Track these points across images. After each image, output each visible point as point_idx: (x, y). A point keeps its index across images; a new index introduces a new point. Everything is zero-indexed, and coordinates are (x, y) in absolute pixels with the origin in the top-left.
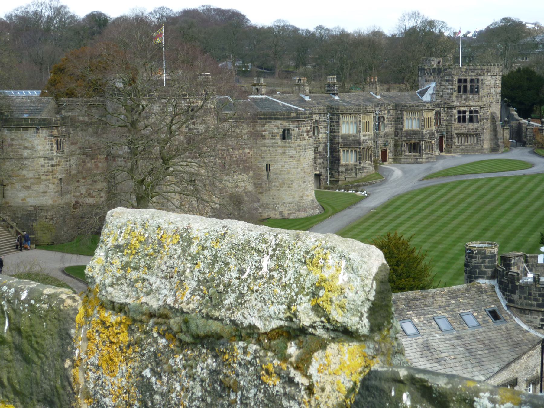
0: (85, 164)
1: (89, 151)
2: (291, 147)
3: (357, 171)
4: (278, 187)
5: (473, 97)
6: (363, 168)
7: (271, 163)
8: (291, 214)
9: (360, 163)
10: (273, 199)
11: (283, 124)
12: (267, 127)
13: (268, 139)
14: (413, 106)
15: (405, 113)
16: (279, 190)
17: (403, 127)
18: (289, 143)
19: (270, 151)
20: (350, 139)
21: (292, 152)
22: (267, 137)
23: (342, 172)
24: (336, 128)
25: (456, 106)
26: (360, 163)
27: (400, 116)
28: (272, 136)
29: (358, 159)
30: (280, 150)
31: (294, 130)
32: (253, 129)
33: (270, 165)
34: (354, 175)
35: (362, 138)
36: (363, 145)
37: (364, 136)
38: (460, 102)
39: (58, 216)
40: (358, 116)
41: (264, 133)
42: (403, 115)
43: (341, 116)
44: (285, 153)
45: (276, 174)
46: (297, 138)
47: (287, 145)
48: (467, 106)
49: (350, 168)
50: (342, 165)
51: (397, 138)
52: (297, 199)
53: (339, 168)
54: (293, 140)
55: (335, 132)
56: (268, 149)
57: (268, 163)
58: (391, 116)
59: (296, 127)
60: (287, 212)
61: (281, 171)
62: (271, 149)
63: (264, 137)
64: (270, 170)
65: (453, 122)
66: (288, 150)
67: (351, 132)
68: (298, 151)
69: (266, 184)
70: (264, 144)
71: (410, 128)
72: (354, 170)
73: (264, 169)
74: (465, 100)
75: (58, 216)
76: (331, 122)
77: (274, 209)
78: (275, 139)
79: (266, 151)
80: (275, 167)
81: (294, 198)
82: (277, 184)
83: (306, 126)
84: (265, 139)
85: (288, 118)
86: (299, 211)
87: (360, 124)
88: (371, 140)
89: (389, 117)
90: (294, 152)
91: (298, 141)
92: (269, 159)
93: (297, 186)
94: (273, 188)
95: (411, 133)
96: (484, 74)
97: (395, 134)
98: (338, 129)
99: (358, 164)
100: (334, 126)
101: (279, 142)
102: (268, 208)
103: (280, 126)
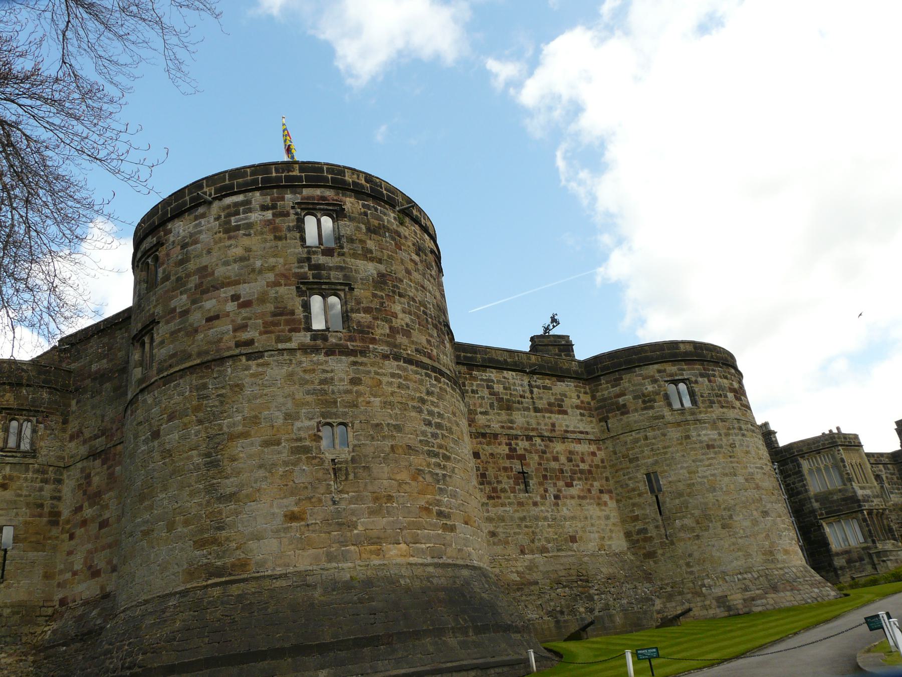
0: (89, 484)
1: (100, 443)
3: (875, 559)
4: (693, 530)
6: (885, 552)
7: (657, 469)
9: (874, 542)
11: (665, 371)
12: (625, 384)
13: (636, 410)
18: (693, 414)
19: (646, 438)
20: (835, 497)
21: (708, 434)
22: (631, 407)
23: (842, 568)
24: (799, 485)
26: (874, 542)
28: (644, 402)
29: (867, 534)
30: (674, 434)
31: (696, 382)
32: (593, 397)
34: (869, 568)
35: (860, 493)
36: (867, 506)
37: (862, 488)
40: (835, 450)
41: (621, 400)
43: (801, 461)
44: (688, 437)
45: (680, 495)
46: (712, 402)
47: (689, 418)
49: (855, 556)
50: (837, 554)
52: (757, 560)
53: (831, 561)
54: (701, 405)
55: (799, 493)
57: (651, 470)
58: (891, 474)
59: (702, 375)
60: (739, 596)
62: (650, 434)
63: (623, 410)
64: (660, 490)
68: (723, 431)
69: (657, 527)
72: (867, 560)
73: (643, 487)
76: (785, 478)
77: (700, 594)
78: (652, 408)
79: (637, 441)
81: (748, 555)
82: (688, 522)
83: (726, 378)
84: (627, 412)
85: (675, 355)
86: (775, 589)
87: (845, 466)
88: (877, 496)
89: (889, 476)
90: (713, 434)
91: (717, 411)
92: (650, 461)
93: (747, 523)
94: (682, 535)
98: (804, 485)
99: (870, 544)
100: (794, 483)
101: (666, 412)
102: (681, 593)
103: (657, 376)
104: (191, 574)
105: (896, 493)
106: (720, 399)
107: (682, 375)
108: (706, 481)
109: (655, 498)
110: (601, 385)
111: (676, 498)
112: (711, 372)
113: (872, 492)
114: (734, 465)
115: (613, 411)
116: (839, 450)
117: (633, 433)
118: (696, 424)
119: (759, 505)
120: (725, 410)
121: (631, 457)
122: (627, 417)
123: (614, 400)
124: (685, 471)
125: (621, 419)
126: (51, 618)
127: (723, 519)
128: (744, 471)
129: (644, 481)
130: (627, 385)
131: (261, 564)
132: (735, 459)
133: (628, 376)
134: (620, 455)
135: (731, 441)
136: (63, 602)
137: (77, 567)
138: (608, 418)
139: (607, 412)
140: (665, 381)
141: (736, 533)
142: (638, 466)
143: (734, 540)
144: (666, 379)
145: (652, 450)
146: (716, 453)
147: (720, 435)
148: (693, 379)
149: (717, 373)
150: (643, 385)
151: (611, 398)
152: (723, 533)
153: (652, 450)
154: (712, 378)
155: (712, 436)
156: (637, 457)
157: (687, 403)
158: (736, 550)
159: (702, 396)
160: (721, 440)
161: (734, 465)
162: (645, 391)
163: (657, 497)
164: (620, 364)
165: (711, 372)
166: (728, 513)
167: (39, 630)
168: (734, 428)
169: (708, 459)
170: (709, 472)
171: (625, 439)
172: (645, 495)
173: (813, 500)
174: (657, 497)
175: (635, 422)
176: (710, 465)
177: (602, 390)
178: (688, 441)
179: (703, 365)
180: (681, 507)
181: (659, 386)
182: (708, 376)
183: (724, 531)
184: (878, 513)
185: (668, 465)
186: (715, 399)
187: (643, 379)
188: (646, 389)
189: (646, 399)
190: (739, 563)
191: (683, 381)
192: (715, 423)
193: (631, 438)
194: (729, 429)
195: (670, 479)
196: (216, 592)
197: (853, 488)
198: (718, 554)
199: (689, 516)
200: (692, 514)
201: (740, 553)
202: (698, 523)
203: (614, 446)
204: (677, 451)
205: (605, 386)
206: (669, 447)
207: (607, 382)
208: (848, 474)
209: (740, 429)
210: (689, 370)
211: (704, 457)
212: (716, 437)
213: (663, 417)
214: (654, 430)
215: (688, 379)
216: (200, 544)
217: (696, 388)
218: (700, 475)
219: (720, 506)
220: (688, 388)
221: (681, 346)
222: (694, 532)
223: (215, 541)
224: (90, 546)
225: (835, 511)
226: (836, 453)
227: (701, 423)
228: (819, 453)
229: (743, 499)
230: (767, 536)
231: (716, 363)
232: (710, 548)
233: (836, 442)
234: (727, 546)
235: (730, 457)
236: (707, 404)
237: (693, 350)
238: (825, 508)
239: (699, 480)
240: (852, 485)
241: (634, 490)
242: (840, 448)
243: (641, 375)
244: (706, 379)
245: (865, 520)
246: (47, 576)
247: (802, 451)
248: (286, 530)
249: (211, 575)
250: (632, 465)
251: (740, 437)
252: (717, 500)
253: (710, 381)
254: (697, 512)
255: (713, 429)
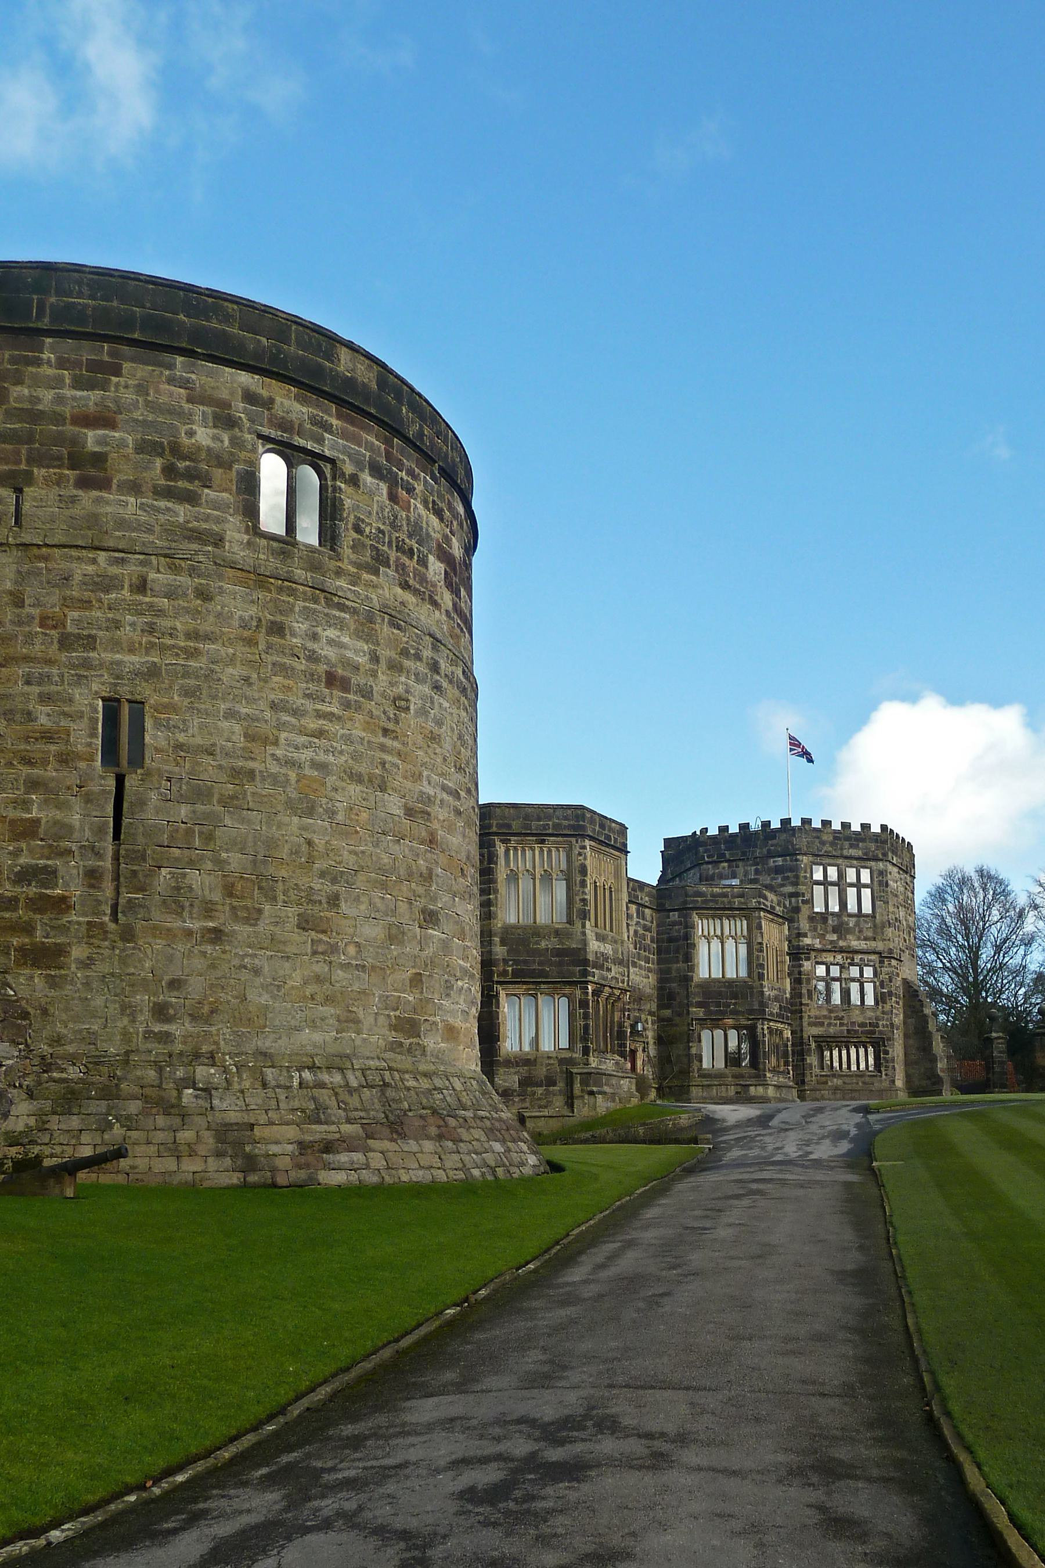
2: (329, 596)
5: (857, 924)
8: (328, 1147)
10: (161, 1012)
13: (134, 488)
14: (725, 895)
15: (696, 918)
16: (217, 935)
17: (692, 969)
18: (315, 567)
19: (141, 586)
20: (543, 944)
22: (123, 473)
25: (811, 949)
27: (677, 931)
28: (169, 471)
29: (579, 1033)
31: (354, 481)
33: (138, 705)
35: (594, 946)
36: (597, 975)
37: (600, 938)
38: (822, 937)
41: (91, 438)
42: (690, 926)
44: (278, 629)
45: (200, 794)
46: (381, 560)
47: (300, 574)
48: (841, 951)
51: (667, 1013)
54: (347, 552)
56: (130, 571)
57: (125, 691)
58: (646, 929)
59: (376, 471)
61: (239, 775)
62: (159, 578)
64: (137, 759)
65: (805, 1001)
66: (308, 614)
67: (542, 919)
68: (386, 653)
70: (93, 520)
71: (717, 974)
74: (834, 931)
78: (191, 498)
79: (105, 584)
80: (193, 735)
81: (349, 1021)
83: (439, 513)
84: (104, 484)
87: (583, 884)
89: (641, 931)
90: (357, 652)
92: (133, 660)
95: (720, 994)
96: (885, 855)
97: (660, 997)
99: (578, 1055)
101: (234, 531)
103: (240, 409)
105: (641, 967)
106: (405, 559)
107: (320, 441)
108: (293, 776)
109: (111, 783)
110: (38, 362)
111: (182, 799)
112: (403, 474)
113: (615, 951)
114: (388, 758)
115: (55, 461)
116: (584, 847)
117: (102, 556)
118: (316, 601)
119: (420, 890)
120: (410, 598)
121: (70, 628)
122: (98, 501)
123: (70, 429)
124: (237, 728)
125: (74, 500)
127: (311, 901)
128: (408, 784)
129: (93, 721)
130: (129, 396)
132: (396, 744)
133: (143, 371)
134: (36, 612)
135: (401, 689)
138: (29, 478)
139: (30, 461)
140: (260, 436)
141: (334, 949)
142: (86, 664)
143: (321, 968)
144: (266, 431)
145: (151, 629)
146: (347, 705)
147: (375, 659)
148: (349, 468)
149: (419, 488)
150: (188, 418)
151: (58, 419)
152: (298, 941)
153: (151, 629)
154: (403, 494)
155: (349, 654)
156: (92, 638)
157: (308, 532)
158: (319, 998)
159: (358, 530)
160: (374, 674)
161: (388, 758)
162: (185, 440)
163: (120, 780)
164: (128, 322)
165: (403, 474)
166: (329, 888)
168: (418, 657)
169: (320, 715)
170: (306, 755)
171: (64, 565)
172: (82, 765)
173: (497, 939)
174: (120, 780)
175: (121, 523)
176: (320, 734)
177: (37, 382)
178: (275, 640)
179: (388, 442)
180: (189, 832)
181: (235, 442)
182: (393, 482)
183: (297, 937)
184: (611, 995)
185: (187, 693)
186: (393, 555)
187: (190, 400)
188: (191, 434)
189: (182, 465)
190: (317, 1037)
191: (316, 460)
192: (371, 620)
193: (90, 569)
194: (404, 653)
195: (181, 738)
197: (584, 934)
198: (265, 999)
199: (209, 865)
200: (220, 863)
201: (328, 1010)
202: (231, 895)
203: (22, 577)
204: (232, 661)
205: (50, 371)
206: (208, 638)
207: (62, 364)
208: (584, 900)
209: (435, 667)
210: (345, 435)
211: (310, 705)
212: (362, 660)
213: (218, 541)
214: (175, 569)
215: (332, 461)
217: (349, 499)
218: (279, 752)
219: (311, 861)
220: (323, 488)
221: (344, 354)
222: (211, 918)
225: (532, 973)
226: (576, 851)
227: (329, 603)
228: (543, 842)
229: (386, 859)
230: (417, 981)
231: (427, 458)
232: (244, 975)
233: (583, 828)
234: (296, 980)
235: (386, 732)
236: (367, 557)
237: (374, 386)
238: (516, 962)
239: (274, 768)
240: (584, 926)
241: (47, 736)
242: (587, 843)
243: (185, 384)
244: (384, 488)
245: (584, 1004)
247: (509, 826)
250: (63, 657)
251: (426, 689)
252: (309, 843)
253: (393, 497)
254: (235, 860)
255: (358, 635)
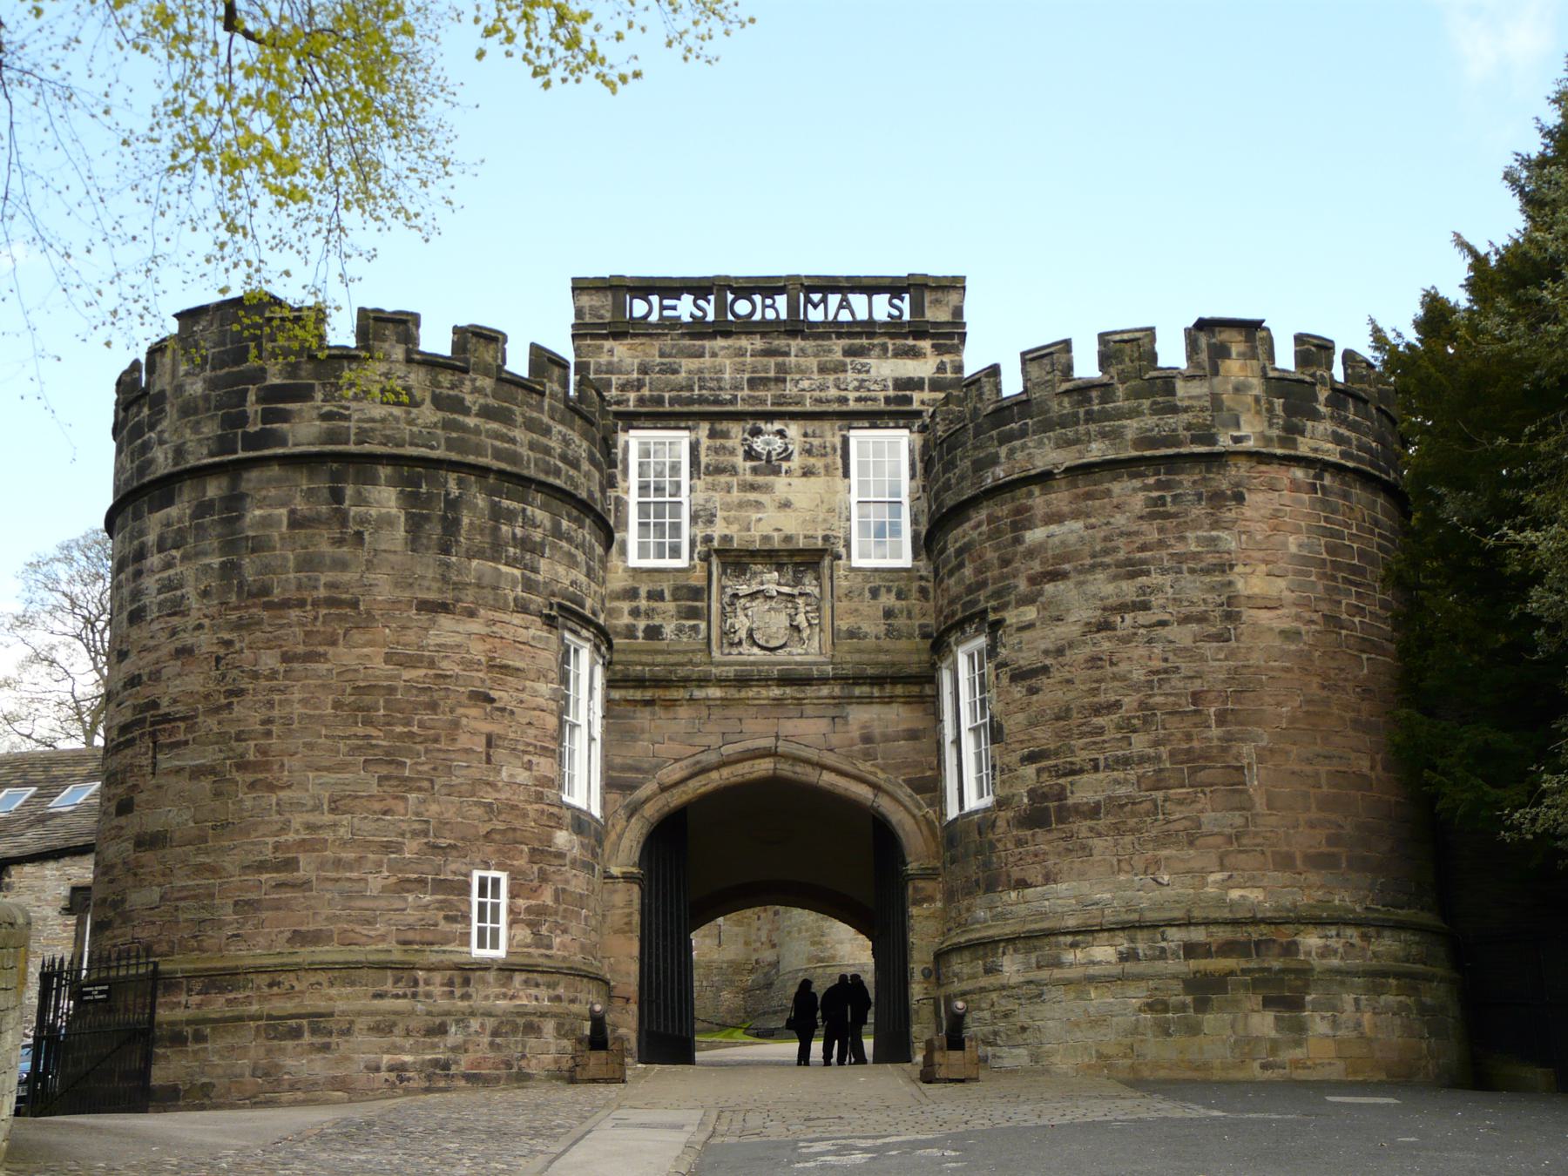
39: (705, 984)
75: (705, 984)
104: (809, 960)
126: (751, 971)
131: (843, 957)
136: (757, 962)
137: (763, 939)
167: (744, 979)
196: (820, 971)
216: (813, 943)
223: (820, 943)
224: (769, 926)
246: (747, 943)
248: (856, 939)
249: (819, 961)
